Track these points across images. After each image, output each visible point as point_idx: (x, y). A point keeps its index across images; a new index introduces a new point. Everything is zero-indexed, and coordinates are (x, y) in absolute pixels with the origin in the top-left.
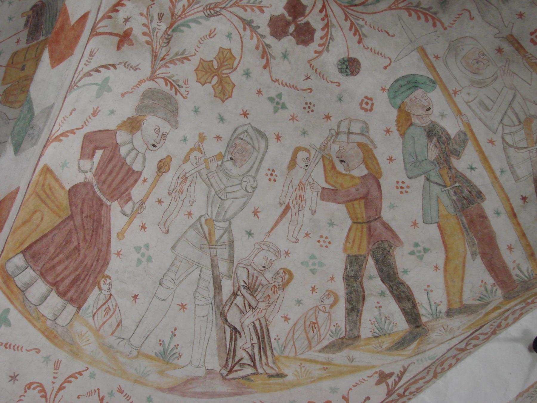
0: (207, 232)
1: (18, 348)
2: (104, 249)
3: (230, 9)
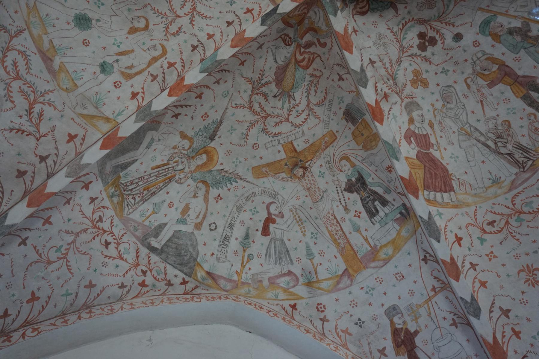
0: (465, 133)
1: (452, 218)
2: (442, 167)
3: (403, 56)
